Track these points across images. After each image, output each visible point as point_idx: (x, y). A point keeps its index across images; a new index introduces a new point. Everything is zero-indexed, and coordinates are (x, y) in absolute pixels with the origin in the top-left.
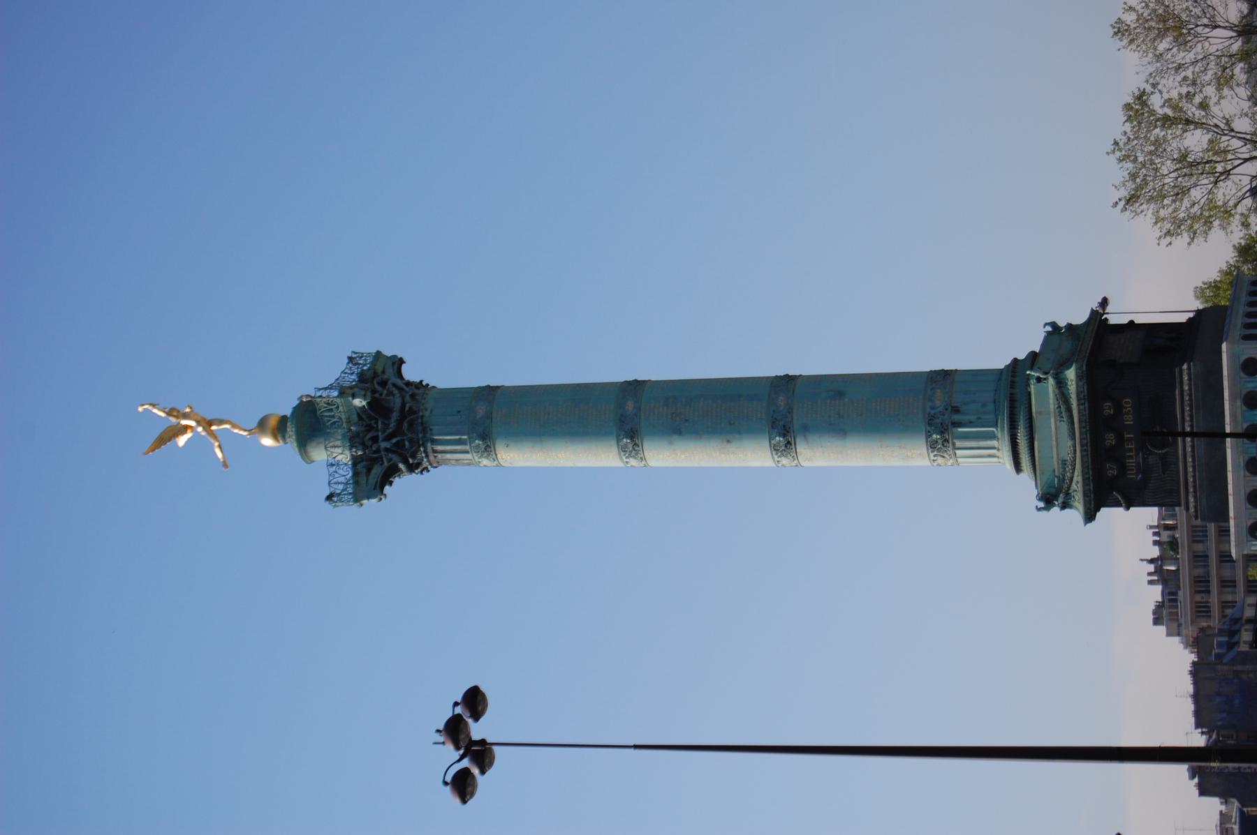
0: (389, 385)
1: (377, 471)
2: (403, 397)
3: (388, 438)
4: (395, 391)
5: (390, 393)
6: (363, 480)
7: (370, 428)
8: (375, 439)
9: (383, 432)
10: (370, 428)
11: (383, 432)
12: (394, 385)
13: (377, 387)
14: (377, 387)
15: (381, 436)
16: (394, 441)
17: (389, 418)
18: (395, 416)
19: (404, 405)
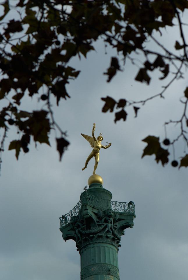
0: (105, 224)
1: (72, 233)
2: (100, 232)
3: (79, 232)
4: (103, 226)
5: (99, 225)
6: (69, 228)
7: (82, 222)
8: (78, 227)
9: (82, 229)
10: (82, 222)
11: (82, 229)
12: (106, 227)
13: (104, 218)
14: (104, 218)
15: (79, 229)
16: (79, 235)
17: (87, 229)
18: (87, 232)
19: (95, 233)
